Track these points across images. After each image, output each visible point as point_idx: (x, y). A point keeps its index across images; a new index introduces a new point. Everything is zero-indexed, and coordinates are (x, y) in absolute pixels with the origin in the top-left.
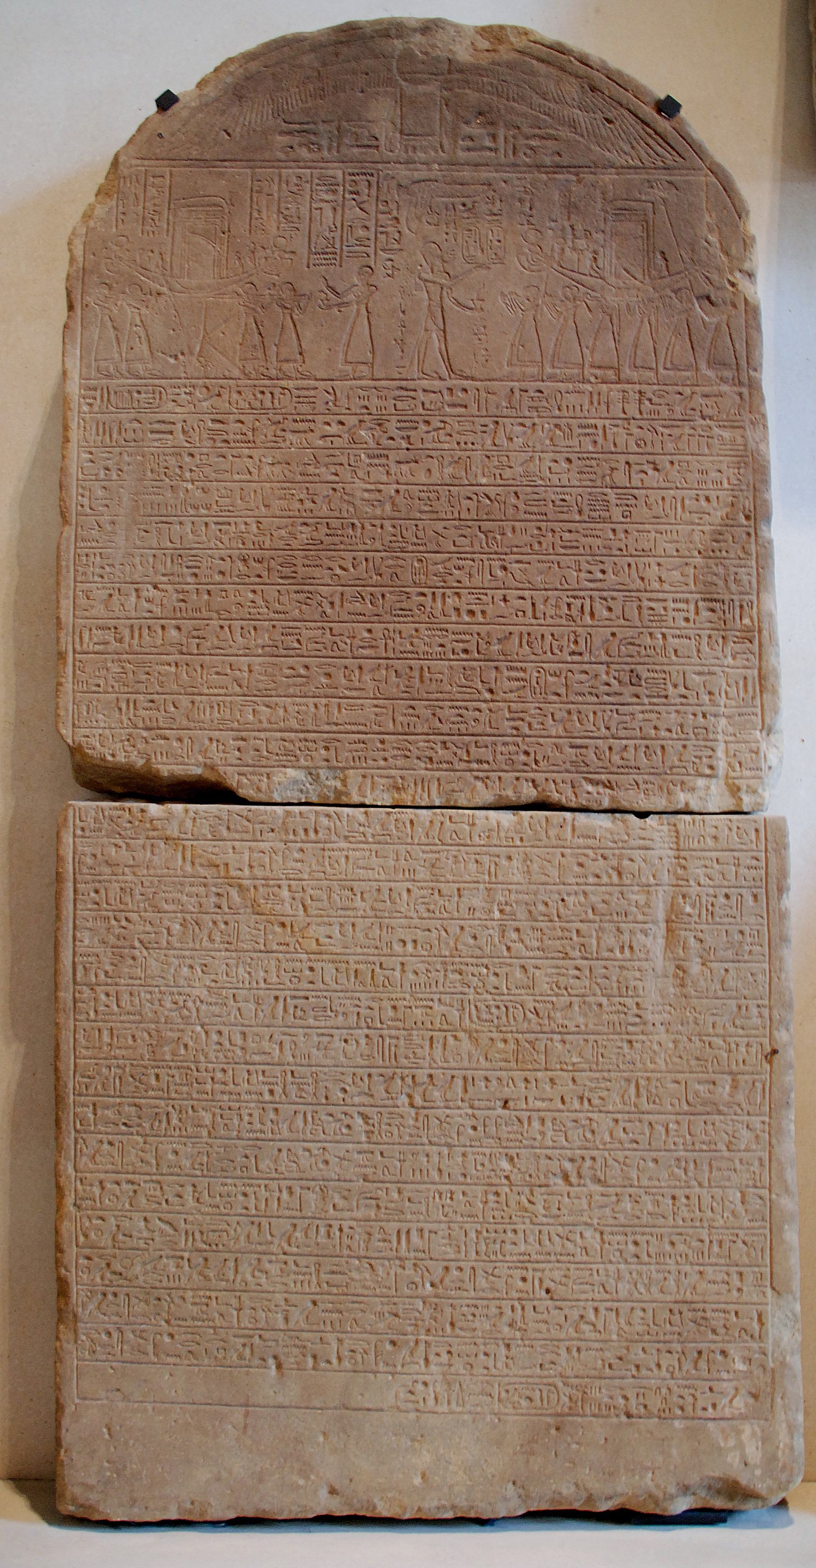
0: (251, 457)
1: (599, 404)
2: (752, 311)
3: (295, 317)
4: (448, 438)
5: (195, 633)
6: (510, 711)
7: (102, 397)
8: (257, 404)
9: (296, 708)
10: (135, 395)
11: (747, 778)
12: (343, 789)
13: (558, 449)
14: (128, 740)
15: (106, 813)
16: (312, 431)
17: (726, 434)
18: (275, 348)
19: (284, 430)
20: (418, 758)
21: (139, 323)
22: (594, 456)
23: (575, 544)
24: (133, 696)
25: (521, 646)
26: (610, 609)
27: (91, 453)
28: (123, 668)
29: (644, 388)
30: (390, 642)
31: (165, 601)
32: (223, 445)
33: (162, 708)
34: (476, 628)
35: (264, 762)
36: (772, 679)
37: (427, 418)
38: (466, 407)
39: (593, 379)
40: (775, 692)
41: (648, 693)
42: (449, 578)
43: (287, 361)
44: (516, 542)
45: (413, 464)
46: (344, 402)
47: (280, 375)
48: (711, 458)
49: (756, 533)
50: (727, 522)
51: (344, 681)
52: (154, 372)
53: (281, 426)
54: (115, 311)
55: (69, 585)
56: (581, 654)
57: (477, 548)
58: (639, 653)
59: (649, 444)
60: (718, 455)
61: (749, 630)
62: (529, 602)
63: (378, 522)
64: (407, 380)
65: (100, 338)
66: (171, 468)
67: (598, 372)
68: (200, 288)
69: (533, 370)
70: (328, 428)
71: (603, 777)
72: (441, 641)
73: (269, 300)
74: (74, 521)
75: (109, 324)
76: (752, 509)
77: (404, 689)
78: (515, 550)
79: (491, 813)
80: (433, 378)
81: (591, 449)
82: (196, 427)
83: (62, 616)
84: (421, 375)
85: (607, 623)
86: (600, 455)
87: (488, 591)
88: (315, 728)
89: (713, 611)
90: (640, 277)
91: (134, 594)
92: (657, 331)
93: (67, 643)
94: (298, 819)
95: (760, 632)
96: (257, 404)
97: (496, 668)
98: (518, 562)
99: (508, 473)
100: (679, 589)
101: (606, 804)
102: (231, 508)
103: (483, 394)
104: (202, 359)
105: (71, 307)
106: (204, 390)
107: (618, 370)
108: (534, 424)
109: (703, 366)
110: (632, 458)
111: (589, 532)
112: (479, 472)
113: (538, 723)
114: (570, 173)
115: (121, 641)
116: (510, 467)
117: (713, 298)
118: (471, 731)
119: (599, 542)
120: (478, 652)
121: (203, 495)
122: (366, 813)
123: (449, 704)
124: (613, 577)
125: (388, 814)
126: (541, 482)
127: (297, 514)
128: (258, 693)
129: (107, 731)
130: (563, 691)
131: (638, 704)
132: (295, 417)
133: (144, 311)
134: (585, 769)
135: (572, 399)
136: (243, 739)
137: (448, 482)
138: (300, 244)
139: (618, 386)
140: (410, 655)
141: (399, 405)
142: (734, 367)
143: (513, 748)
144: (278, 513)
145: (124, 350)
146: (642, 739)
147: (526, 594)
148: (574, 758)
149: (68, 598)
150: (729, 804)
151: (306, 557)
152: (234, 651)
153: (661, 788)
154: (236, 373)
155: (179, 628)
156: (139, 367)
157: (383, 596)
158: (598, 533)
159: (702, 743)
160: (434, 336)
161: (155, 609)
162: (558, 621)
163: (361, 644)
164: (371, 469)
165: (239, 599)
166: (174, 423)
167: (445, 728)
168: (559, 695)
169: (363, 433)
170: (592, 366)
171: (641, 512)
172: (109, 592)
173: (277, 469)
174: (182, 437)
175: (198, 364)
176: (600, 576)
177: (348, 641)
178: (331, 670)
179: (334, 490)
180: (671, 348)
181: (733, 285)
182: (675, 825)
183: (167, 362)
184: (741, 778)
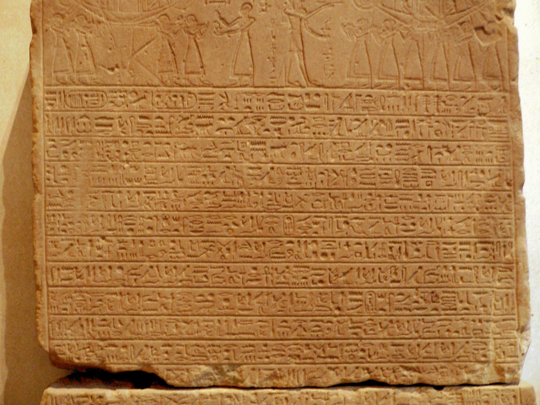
0: (168, 144)
1: (410, 104)
2: (512, 39)
3: (198, 41)
4: (307, 130)
5: (133, 272)
6: (352, 322)
7: (60, 98)
8: (173, 105)
9: (206, 323)
10: (85, 98)
11: (508, 363)
12: (240, 378)
13: (382, 137)
14: (89, 347)
15: (76, 400)
16: (211, 124)
17: (496, 126)
18: (183, 64)
19: (191, 124)
20: (290, 356)
21: (85, 43)
22: (408, 142)
23: (394, 205)
24: (92, 317)
25: (359, 277)
26: (418, 250)
27: (54, 140)
28: (83, 296)
29: (441, 93)
30: (269, 276)
31: (111, 249)
32: (149, 135)
33: (112, 325)
34: (328, 265)
35: (185, 361)
36: (525, 295)
37: (292, 115)
38: (319, 107)
39: (406, 88)
40: (527, 305)
41: (443, 307)
42: (309, 230)
43: (193, 73)
44: (354, 204)
45: (283, 149)
46: (233, 103)
47: (188, 83)
48: (485, 143)
49: (515, 196)
50: (496, 188)
51: (238, 305)
52: (98, 81)
53: (189, 121)
54: (68, 35)
55: (41, 238)
56: (399, 282)
57: (328, 209)
58: (437, 280)
59: (444, 133)
60: (490, 141)
61: (509, 262)
62: (364, 246)
63: (259, 191)
64: (278, 87)
65: (57, 55)
66: (112, 152)
67: (409, 82)
68: (130, 19)
69: (363, 80)
70: (222, 122)
71: (414, 365)
72: (305, 275)
73: (178, 28)
74: (43, 191)
75: (64, 44)
76: (512, 178)
77: (280, 309)
78: (354, 210)
79: (340, 391)
80: (297, 86)
81: (405, 137)
82: (129, 122)
83: (37, 260)
84: (288, 84)
85: (416, 260)
86: (412, 142)
87: (336, 239)
88: (219, 337)
89: (485, 249)
90: (436, 13)
91: (89, 244)
92: (449, 53)
93: (42, 278)
94: (209, 400)
95: (517, 263)
96: (173, 105)
97: (342, 293)
98: (356, 218)
99: (349, 155)
100: (464, 235)
101: (415, 381)
102: (156, 181)
103: (330, 97)
104: (131, 71)
105: (35, 31)
106: (134, 94)
107: (422, 79)
108: (366, 120)
109: (480, 78)
110: (433, 144)
111: (404, 197)
112: (329, 154)
113: (371, 330)
115: (79, 277)
116: (350, 151)
117: (486, 29)
118: (326, 336)
119: (410, 203)
120: (330, 282)
121: (135, 172)
122: (256, 394)
123: (311, 318)
124: (421, 228)
125: (271, 394)
126: (371, 161)
127: (203, 185)
128: (178, 313)
129: (74, 342)
130: (387, 307)
131: (437, 315)
132: (200, 114)
133: (89, 35)
134: (402, 360)
135: (392, 101)
136: (169, 345)
137: (309, 162)
139: (423, 92)
140: (283, 285)
141: (273, 105)
142: (501, 78)
143: (354, 348)
144: (189, 185)
145: (75, 63)
146: (439, 338)
147: (362, 241)
148: (395, 353)
149: (41, 247)
150: (496, 378)
151: (210, 216)
152: (162, 284)
153: (452, 371)
154: (156, 81)
155: (121, 268)
156: (86, 77)
157: (264, 243)
158: (410, 197)
159: (479, 340)
160: (296, 55)
161: (104, 255)
162: (384, 259)
163: (249, 277)
164: (254, 152)
165: (163, 247)
166: (112, 119)
167: (308, 335)
168: (384, 310)
169: (248, 127)
170: (406, 78)
171: (440, 182)
172: (70, 242)
173: (187, 153)
174: (120, 129)
175: (128, 75)
176: (412, 227)
177: (241, 276)
178: (230, 296)
179: (228, 167)
180: (458, 65)
181: (499, 19)
182: (461, 394)
183: (105, 72)
184: (504, 362)
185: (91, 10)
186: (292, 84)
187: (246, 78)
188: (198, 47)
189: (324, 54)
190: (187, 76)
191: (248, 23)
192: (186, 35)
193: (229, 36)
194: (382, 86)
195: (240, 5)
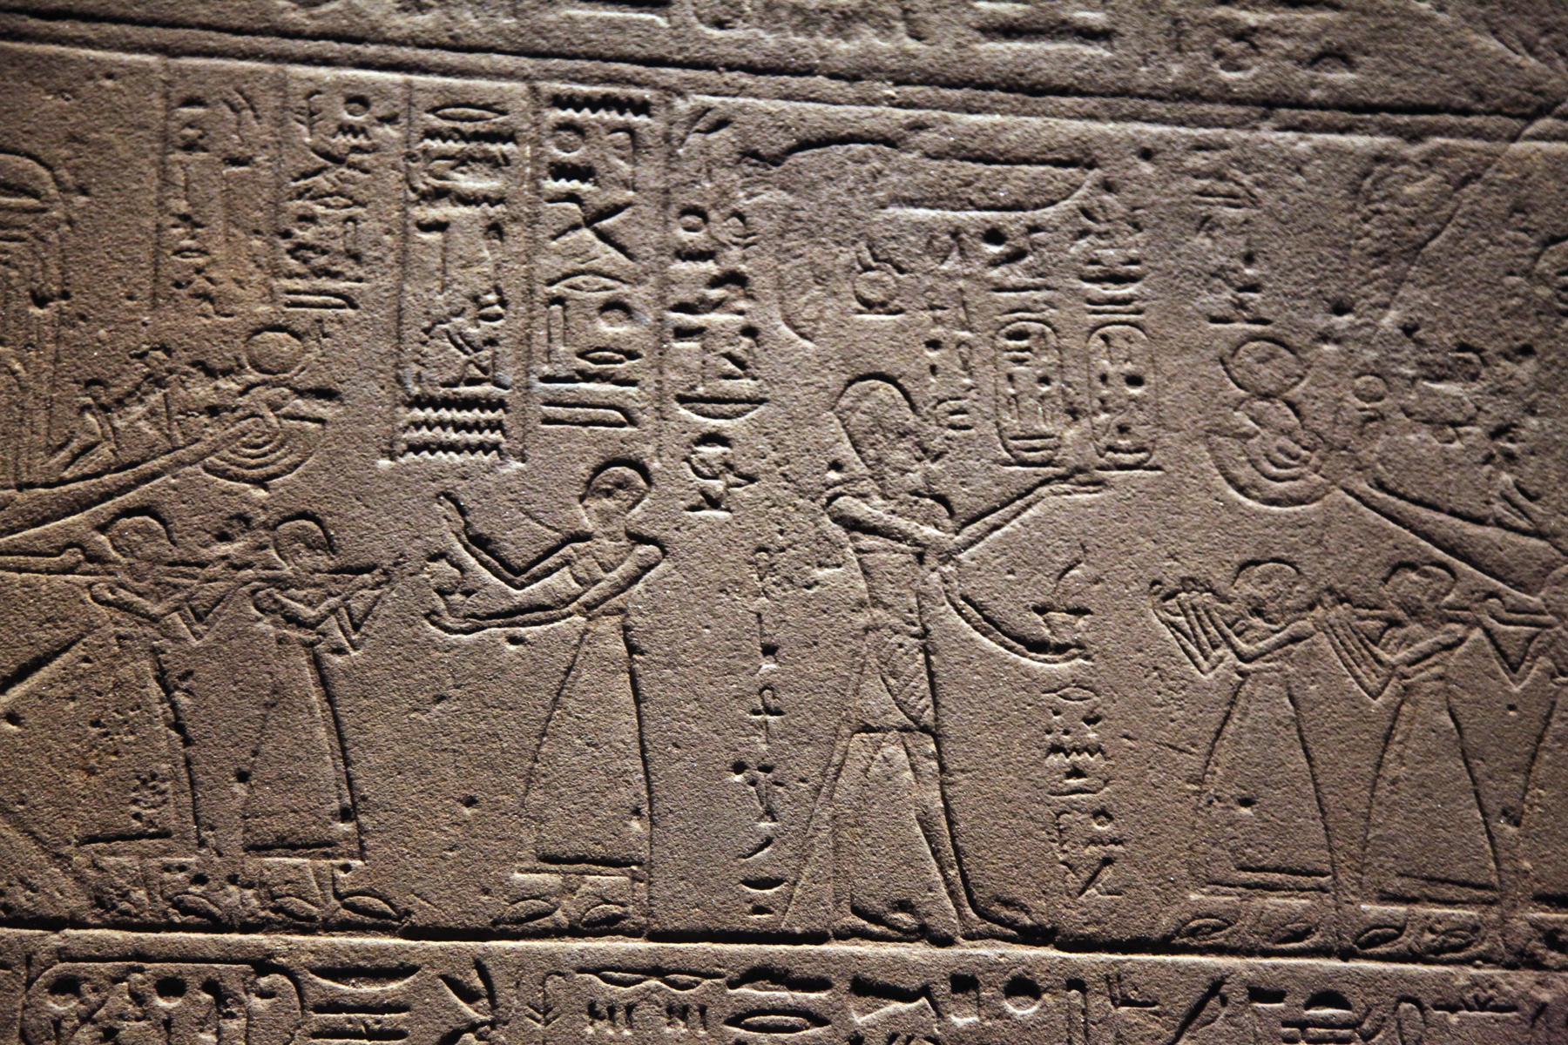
73: (220, 586)
80: (908, 936)
103: (1099, 1003)
114: (1386, 129)
186: (876, 919)
187: (611, 880)
188: (330, 698)
189: (1055, 749)
190: (252, 864)
191: (628, 567)
192: (265, 625)
193: (513, 640)
194: (1405, 941)
195: (583, 469)
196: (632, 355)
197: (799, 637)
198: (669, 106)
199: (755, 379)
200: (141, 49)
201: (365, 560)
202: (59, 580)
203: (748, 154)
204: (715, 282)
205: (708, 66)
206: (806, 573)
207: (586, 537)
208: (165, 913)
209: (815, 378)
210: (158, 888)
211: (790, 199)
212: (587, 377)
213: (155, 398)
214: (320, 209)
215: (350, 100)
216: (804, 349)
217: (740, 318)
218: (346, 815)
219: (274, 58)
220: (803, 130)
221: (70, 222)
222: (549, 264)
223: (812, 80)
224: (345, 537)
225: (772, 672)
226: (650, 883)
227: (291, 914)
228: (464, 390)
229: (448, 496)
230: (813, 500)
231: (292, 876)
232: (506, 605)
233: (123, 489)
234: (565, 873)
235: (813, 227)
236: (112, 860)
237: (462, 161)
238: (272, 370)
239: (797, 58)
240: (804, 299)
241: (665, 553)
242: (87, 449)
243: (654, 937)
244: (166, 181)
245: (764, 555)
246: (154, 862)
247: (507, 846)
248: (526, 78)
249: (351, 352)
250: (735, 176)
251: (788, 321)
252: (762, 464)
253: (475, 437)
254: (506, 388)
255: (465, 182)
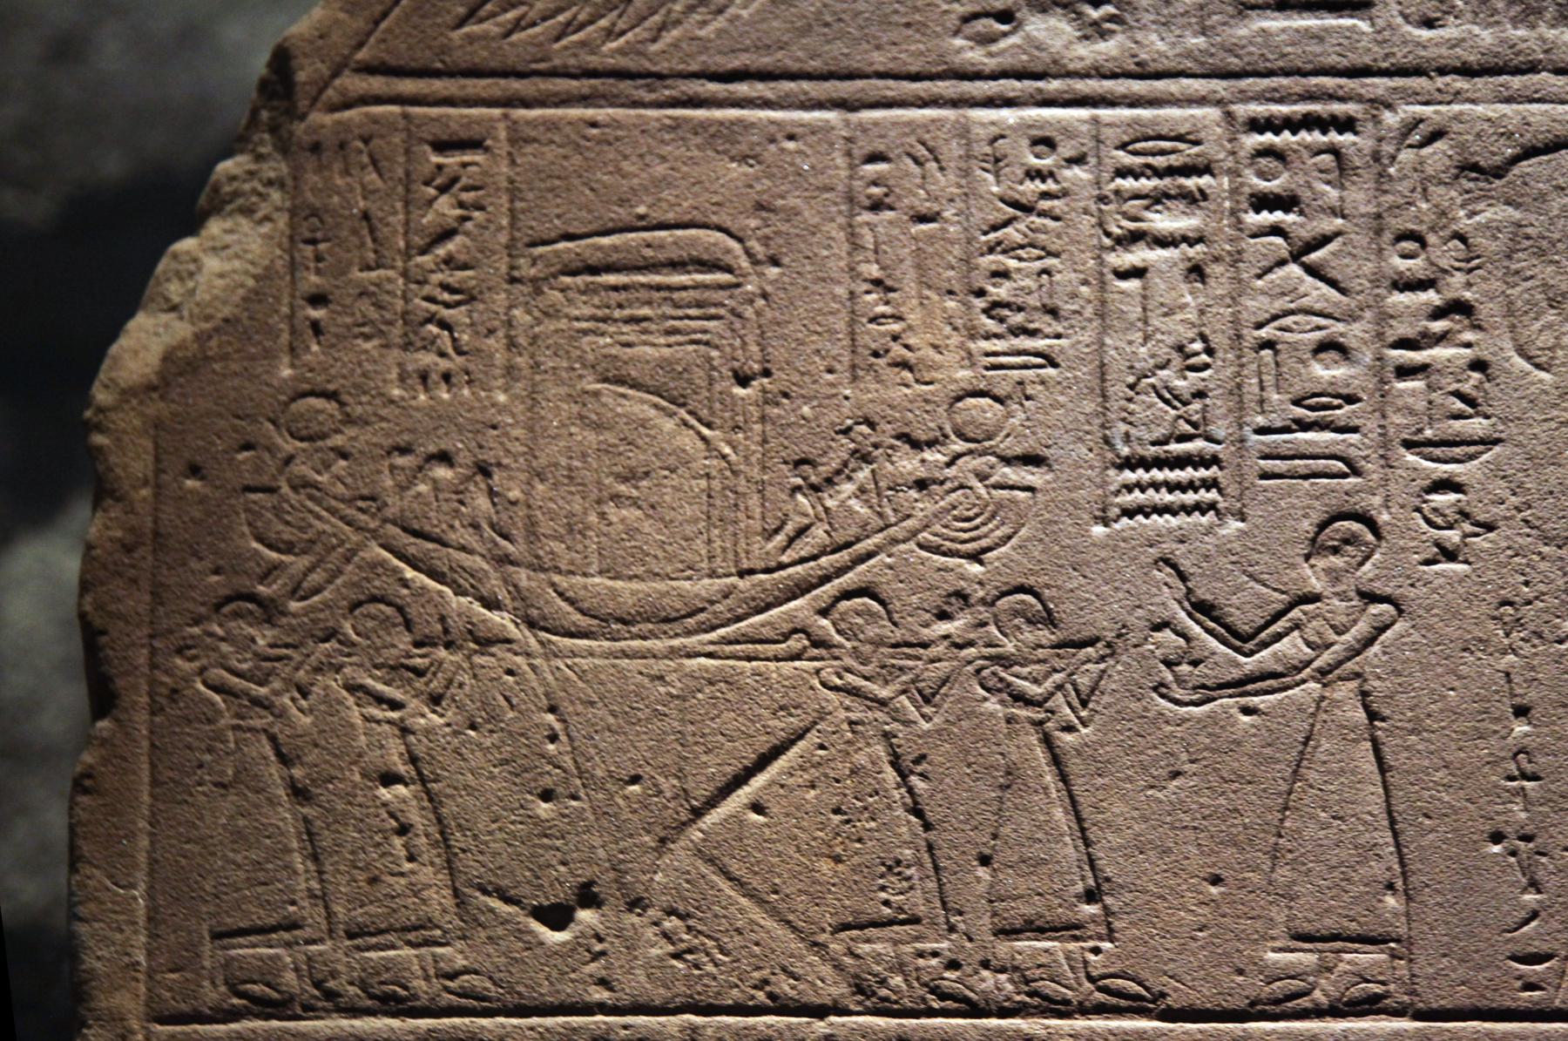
43: (1036, 928)
75: (274, 771)
138: (1057, 412)
183: (521, 932)
185: (433, 574)
187: (1369, 958)
188: (1064, 777)
190: (1003, 948)
191: (1362, 628)
192: (992, 705)
193: (1247, 711)
195: (1307, 526)
196: (1351, 399)
197: (1554, 696)
198: (1376, 120)
199: (1487, 417)
200: (820, 105)
201: (1087, 633)
202: (787, 667)
203: (1468, 168)
204: (1438, 313)
205: (1418, 71)
206: (1557, 627)
207: (1314, 598)
208: (924, 1000)
209: (1555, 413)
210: (914, 974)
211: (1517, 215)
212: (1305, 426)
213: (864, 474)
214: (1013, 264)
215: (1036, 142)
216: (1541, 381)
217: (1468, 351)
218: (1091, 896)
219: (955, 103)
220: (1528, 136)
221: (765, 296)
222: (1256, 306)
223: (1536, 78)
224: (1064, 610)
225: (1526, 735)
226: (1411, 961)
227: (1046, 998)
228: (1176, 448)
229: (1167, 562)
230: (1560, 547)
231: (1043, 960)
232: (1236, 674)
233: (841, 571)
234: (1321, 952)
235: (1545, 244)
236: (867, 947)
237: (1157, 199)
238: (977, 438)
239: (1517, 54)
240: (1538, 325)
241: (1400, 612)
242: (802, 531)
243: (1419, 1016)
244: (856, 246)
245: (1510, 610)
246: (908, 949)
247: (1259, 924)
248: (1219, 102)
249: (1057, 412)
250: (1453, 194)
251: (1521, 351)
252: (1500, 510)
253: (1190, 497)
254: (1218, 442)
255: (1161, 222)
